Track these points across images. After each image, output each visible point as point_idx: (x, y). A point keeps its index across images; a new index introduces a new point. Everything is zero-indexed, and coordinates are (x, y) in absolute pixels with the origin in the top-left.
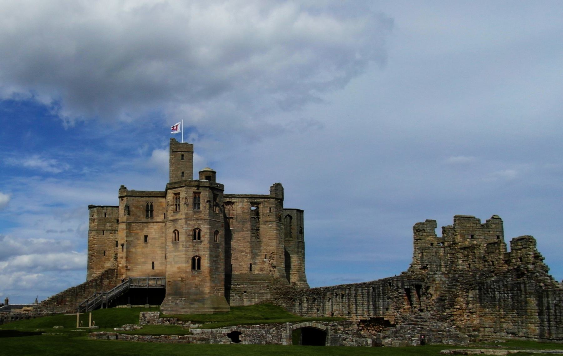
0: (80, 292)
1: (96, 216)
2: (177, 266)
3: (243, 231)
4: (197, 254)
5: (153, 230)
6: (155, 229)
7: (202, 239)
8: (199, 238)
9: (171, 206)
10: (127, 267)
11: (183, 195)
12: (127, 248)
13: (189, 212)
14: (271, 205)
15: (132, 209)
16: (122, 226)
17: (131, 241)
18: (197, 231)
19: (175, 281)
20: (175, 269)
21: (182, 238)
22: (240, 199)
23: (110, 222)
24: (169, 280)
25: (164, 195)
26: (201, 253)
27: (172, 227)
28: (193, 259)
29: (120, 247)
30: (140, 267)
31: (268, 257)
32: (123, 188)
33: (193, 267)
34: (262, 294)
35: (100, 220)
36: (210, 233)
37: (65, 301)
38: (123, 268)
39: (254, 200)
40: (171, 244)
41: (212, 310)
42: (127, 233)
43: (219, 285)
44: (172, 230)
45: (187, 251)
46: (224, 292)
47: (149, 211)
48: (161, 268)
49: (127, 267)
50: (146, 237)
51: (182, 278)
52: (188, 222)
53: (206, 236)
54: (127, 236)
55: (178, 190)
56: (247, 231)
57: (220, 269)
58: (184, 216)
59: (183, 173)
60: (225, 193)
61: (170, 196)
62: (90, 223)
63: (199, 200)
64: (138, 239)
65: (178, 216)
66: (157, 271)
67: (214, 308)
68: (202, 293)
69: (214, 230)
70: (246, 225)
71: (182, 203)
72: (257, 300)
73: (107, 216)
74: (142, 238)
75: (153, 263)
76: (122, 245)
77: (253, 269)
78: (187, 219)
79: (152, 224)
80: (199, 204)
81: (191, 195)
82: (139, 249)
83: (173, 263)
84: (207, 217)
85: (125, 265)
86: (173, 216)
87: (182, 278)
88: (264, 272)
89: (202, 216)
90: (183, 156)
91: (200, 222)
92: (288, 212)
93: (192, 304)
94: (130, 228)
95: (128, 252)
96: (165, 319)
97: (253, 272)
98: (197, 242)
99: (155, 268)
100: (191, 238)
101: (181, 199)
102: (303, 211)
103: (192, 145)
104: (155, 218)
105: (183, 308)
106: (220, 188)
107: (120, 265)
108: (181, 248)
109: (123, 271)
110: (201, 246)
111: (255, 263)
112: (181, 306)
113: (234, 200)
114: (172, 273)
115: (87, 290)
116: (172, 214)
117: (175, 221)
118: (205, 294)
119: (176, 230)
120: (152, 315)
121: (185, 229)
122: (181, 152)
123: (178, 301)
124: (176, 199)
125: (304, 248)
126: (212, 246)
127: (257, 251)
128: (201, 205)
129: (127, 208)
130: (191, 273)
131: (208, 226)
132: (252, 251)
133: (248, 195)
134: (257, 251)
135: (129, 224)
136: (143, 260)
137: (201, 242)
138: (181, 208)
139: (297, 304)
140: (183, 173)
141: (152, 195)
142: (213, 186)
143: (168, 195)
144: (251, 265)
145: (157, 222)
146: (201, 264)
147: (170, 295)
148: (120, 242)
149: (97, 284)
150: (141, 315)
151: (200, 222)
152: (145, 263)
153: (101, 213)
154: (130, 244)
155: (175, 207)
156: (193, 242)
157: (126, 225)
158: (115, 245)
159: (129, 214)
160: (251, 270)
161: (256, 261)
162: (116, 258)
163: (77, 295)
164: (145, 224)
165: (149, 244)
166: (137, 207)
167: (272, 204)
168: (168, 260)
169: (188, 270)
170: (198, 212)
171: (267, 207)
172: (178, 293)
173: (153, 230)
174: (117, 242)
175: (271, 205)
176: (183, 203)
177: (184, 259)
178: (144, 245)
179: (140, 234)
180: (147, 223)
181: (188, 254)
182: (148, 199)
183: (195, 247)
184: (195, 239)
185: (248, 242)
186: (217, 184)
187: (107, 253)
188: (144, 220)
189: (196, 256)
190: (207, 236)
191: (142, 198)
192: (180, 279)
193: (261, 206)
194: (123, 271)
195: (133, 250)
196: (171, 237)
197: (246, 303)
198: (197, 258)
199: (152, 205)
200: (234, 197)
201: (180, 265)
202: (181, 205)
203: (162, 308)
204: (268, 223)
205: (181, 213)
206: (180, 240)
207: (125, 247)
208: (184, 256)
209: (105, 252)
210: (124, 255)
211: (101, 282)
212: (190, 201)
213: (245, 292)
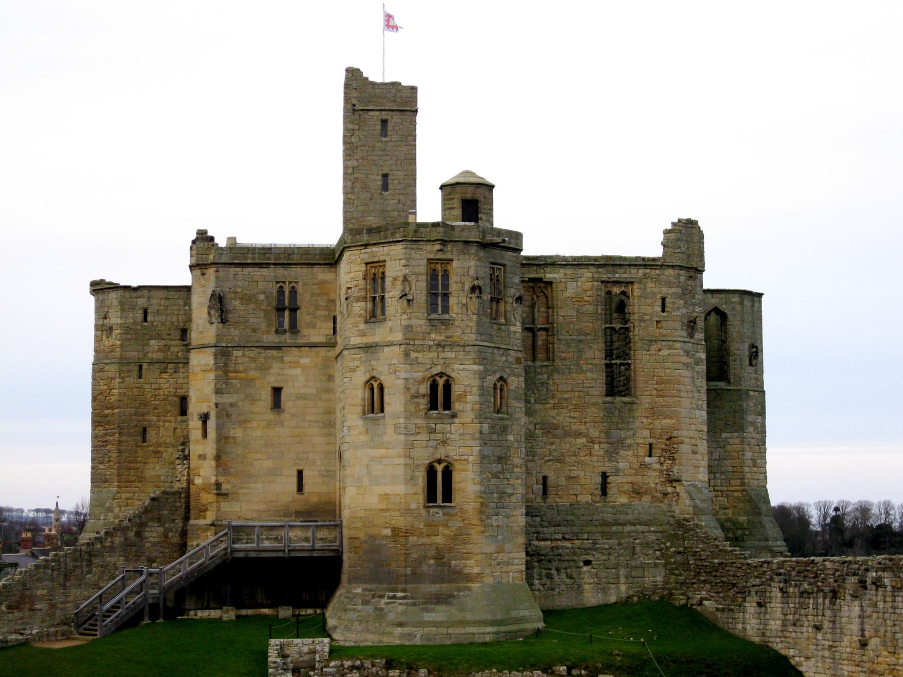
0: (75, 567)
1: (115, 319)
2: (380, 490)
3: (580, 371)
4: (441, 453)
5: (298, 371)
6: (304, 368)
7: (457, 406)
8: (447, 405)
9: (358, 300)
10: (218, 485)
11: (394, 270)
12: (219, 428)
13: (414, 322)
15: (235, 305)
16: (202, 360)
17: (232, 405)
18: (441, 382)
19: (373, 537)
20: (372, 501)
21: (395, 403)
22: (569, 271)
23: (159, 337)
24: (353, 533)
25: (329, 258)
26: (452, 452)
27: (362, 368)
28: (431, 472)
29: (195, 424)
30: (259, 485)
32: (203, 239)
33: (431, 497)
34: (643, 566)
35: (127, 330)
36: (482, 387)
37: (33, 599)
38: (205, 488)
39: (614, 276)
40: (360, 423)
41: (490, 629)
42: (217, 378)
43: (507, 546)
44: (360, 378)
45: (409, 446)
46: (523, 567)
47: (286, 307)
48: (323, 489)
49: (218, 485)
50: (277, 391)
51: (394, 530)
52: (413, 355)
53: (469, 398)
54: (218, 392)
55: (380, 252)
56: (591, 371)
57: (513, 499)
58: (398, 336)
60: (523, 253)
61: (350, 271)
62: (98, 340)
63: (446, 286)
64: (253, 400)
65: (380, 334)
66: (314, 499)
67: (492, 623)
68: (459, 576)
69: (492, 379)
70: (589, 354)
71: (392, 294)
72: (623, 588)
73: (149, 318)
74: (266, 396)
75: (300, 473)
76: (205, 418)
77: (612, 490)
78: (410, 344)
79: (295, 351)
80: (446, 296)
81: (423, 270)
82: (257, 430)
83: (366, 481)
84: (471, 338)
85: (213, 479)
86: (363, 334)
87: (394, 530)
88: (646, 499)
89: (456, 333)
90: (384, 122)
91: (450, 355)
92: (714, 301)
93: (427, 610)
94: (226, 365)
95: (223, 439)
96: (348, 663)
98: (440, 417)
99: (306, 489)
100: (424, 403)
101: (388, 281)
102: (760, 295)
103: (414, 90)
104: (305, 331)
105: (401, 625)
106: (510, 242)
107: (198, 481)
108: (390, 435)
109: (207, 498)
110: (454, 430)
111: (617, 472)
112: (391, 616)
113: (550, 275)
114: (362, 514)
115: (97, 561)
116: (362, 326)
117: (369, 348)
118: (469, 578)
119: (373, 378)
120: (305, 649)
121: (403, 375)
122: (379, 116)
123: (383, 601)
124: (374, 279)
125: (762, 413)
126: (486, 427)
127: (623, 434)
128: (453, 301)
129: (219, 302)
130: (423, 512)
131: (476, 367)
132: (607, 433)
133: (596, 259)
134: (623, 434)
135: (223, 353)
136: (268, 464)
137: (454, 416)
138: (389, 311)
139: (751, 607)
140: (385, 176)
141: (296, 258)
142: (489, 238)
143: (343, 266)
145: (312, 346)
146: (456, 485)
147: (354, 579)
148: (195, 407)
149: (128, 544)
150: (273, 656)
151: (450, 355)
152: (273, 473)
153: (133, 308)
154: (228, 416)
155: (369, 305)
156: (427, 417)
157: (215, 355)
158: (177, 410)
159: (223, 321)
160: (604, 492)
161: (621, 465)
162: (187, 457)
163: (66, 577)
164: (274, 353)
165: (285, 416)
166: (248, 299)
167: (669, 284)
168: (349, 471)
169: (413, 506)
170: (446, 323)
171: (654, 294)
172: (383, 575)
173: (297, 373)
174: (184, 400)
175: (664, 290)
176: (398, 293)
177: (400, 471)
178: (270, 416)
179: (258, 383)
180: (278, 348)
181: (414, 453)
182: (281, 272)
183: (433, 431)
184: (433, 406)
185: (594, 404)
186: (500, 232)
187: (152, 435)
188: (272, 338)
189: (439, 461)
190: (473, 398)
191: (264, 271)
192: (388, 532)
193: (636, 290)
194: (207, 498)
195: (237, 433)
196: (359, 401)
197: (591, 597)
198: (439, 468)
199: (293, 292)
200: (553, 264)
201: (389, 489)
202: (388, 301)
203: (331, 622)
204: (654, 347)
205: (389, 324)
206: (387, 408)
207: (212, 423)
208: (402, 461)
209: (145, 430)
210: (209, 447)
211: (138, 534)
212: (419, 288)
213: (587, 563)
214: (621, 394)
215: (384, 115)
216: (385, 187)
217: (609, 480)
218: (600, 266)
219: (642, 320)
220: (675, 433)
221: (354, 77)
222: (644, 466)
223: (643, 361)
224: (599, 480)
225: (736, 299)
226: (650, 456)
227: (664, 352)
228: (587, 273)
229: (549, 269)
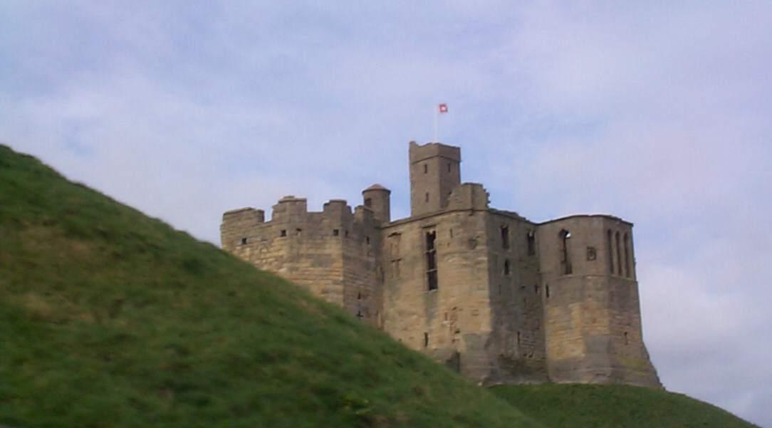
14: (452, 225)
31: (449, 318)
59: (427, 195)
97: (429, 347)
111: (431, 331)
132: (426, 310)
140: (427, 195)
144: (426, 335)
175: (452, 225)
204: (446, 258)
214: (434, 288)
215: (425, 162)
216: (427, 200)
217: (429, 336)
218: (421, 219)
219: (440, 245)
220: (457, 306)
221: (412, 144)
222: (443, 326)
223: (443, 267)
224: (424, 337)
225: (571, 221)
226: (446, 319)
227: (450, 261)
228: (416, 225)
229: (400, 227)
